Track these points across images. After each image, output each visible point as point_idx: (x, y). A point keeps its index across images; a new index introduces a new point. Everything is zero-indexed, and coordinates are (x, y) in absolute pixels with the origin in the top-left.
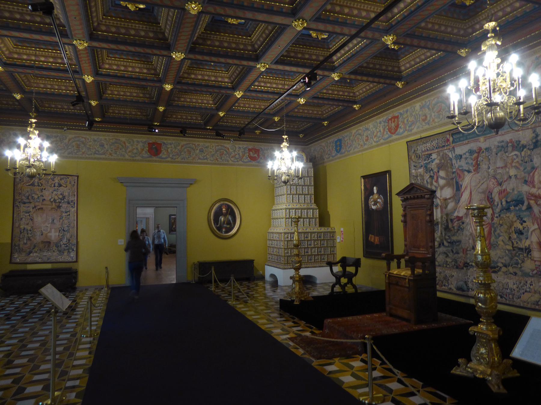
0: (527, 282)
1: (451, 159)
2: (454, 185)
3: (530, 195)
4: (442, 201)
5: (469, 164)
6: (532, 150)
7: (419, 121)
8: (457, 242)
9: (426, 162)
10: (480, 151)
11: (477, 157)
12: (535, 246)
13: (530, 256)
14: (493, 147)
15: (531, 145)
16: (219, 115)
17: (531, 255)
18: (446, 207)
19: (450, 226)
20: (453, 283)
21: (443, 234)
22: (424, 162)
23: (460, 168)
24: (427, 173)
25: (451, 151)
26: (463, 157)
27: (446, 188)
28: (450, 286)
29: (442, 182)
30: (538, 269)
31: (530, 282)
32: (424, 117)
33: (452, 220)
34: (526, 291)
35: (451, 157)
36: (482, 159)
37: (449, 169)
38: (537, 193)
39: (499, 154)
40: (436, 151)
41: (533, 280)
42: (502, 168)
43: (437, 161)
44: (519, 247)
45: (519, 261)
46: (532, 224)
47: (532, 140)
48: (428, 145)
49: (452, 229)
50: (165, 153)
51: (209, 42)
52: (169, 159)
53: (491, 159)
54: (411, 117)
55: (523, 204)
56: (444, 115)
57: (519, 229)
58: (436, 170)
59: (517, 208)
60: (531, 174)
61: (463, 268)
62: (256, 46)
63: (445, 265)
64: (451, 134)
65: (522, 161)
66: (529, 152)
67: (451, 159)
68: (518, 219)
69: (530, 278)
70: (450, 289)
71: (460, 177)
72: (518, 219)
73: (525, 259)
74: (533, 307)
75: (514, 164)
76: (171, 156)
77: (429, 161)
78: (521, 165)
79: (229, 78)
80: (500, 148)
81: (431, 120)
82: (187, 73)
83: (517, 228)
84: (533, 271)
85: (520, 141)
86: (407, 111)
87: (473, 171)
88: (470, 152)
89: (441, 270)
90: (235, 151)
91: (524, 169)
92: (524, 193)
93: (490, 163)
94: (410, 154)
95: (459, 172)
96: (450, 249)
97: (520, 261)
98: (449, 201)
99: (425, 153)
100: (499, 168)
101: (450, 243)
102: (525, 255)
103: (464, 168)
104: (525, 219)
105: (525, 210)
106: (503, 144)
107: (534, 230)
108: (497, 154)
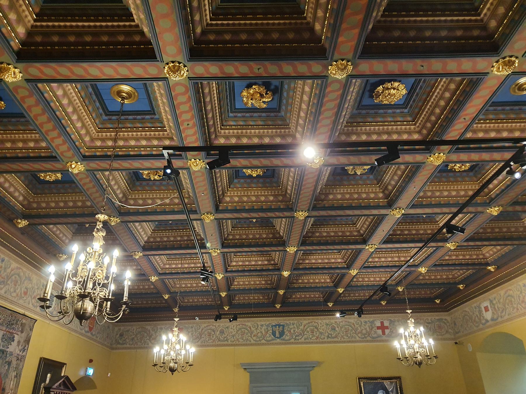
16: (338, 291)
50: (288, 334)
51: (317, 234)
52: (293, 340)
62: (362, 232)
76: (294, 337)
79: (343, 259)
82: (302, 260)
90: (360, 326)
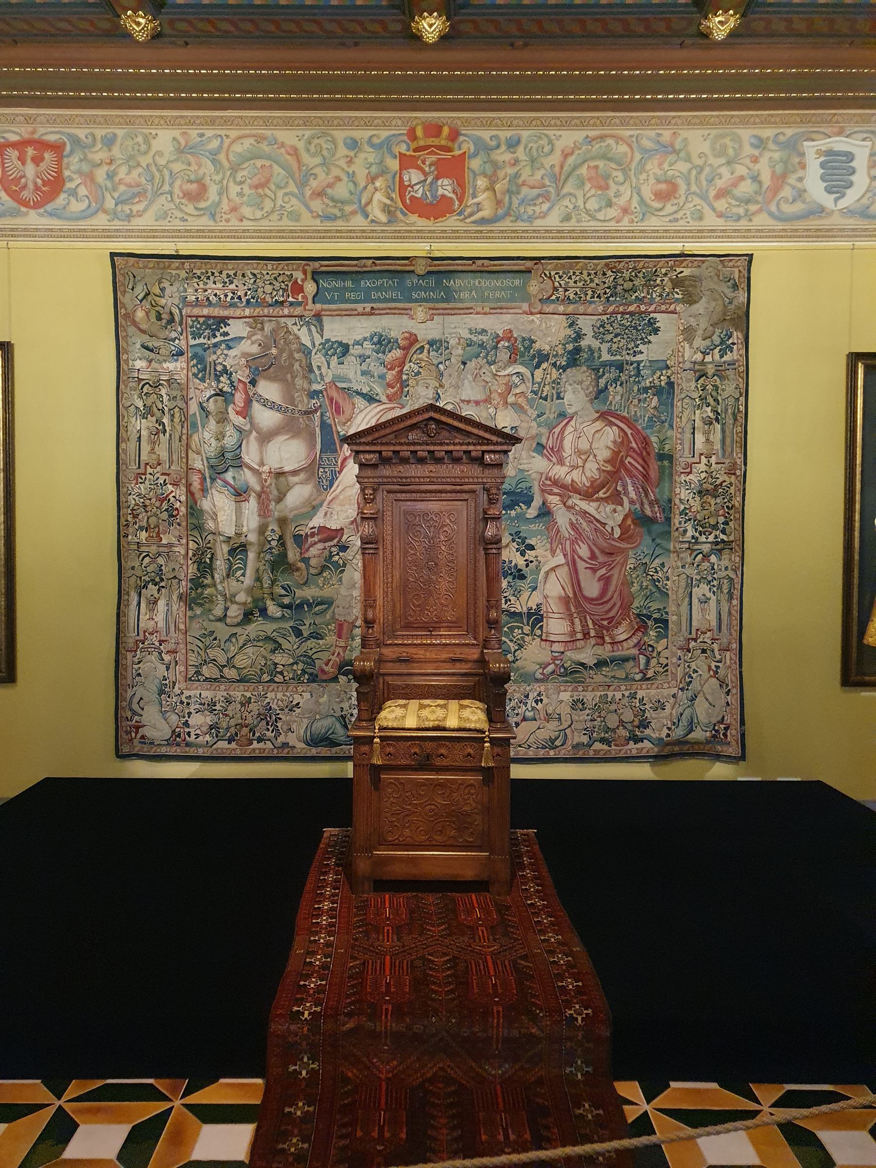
0: (527, 696)
1: (307, 352)
2: (312, 435)
3: (549, 482)
4: (264, 476)
5: (373, 376)
6: (564, 369)
7: (171, 193)
8: (318, 604)
9: (202, 340)
10: (411, 344)
11: (403, 364)
12: (555, 606)
13: (538, 632)
14: (453, 342)
15: (562, 355)
17: (541, 628)
18: (280, 500)
19: (293, 554)
20: (294, 726)
21: (266, 583)
22: (192, 342)
23: (340, 385)
24: (203, 380)
25: (308, 324)
26: (355, 351)
27: (281, 438)
28: (281, 739)
29: (266, 418)
30: (558, 662)
31: (536, 694)
32: (194, 187)
33: (299, 540)
34: (524, 719)
35: (309, 344)
36: (416, 368)
37: (299, 382)
38: (568, 480)
39: (471, 365)
40: (247, 312)
41: (542, 688)
42: (477, 403)
43: (250, 347)
44: (513, 610)
45: (511, 644)
46: (548, 554)
47: (564, 345)
48: (211, 284)
49: (301, 565)
53: (445, 374)
54: (131, 168)
55: (529, 502)
56: (279, 202)
57: (516, 565)
58: (242, 375)
59: (513, 513)
60: (557, 430)
61: (335, 679)
63: (266, 677)
64: (309, 269)
65: (535, 393)
66: (555, 374)
67: (307, 352)
68: (513, 540)
69: (536, 685)
70: (285, 745)
71: (338, 410)
72: (513, 540)
73: (527, 638)
74: (541, 753)
75: (511, 399)
77: (214, 341)
78: (530, 402)
80: (475, 349)
81: (225, 206)
83: (511, 562)
84: (544, 666)
85: (534, 342)
86: (109, 142)
87: (384, 399)
88: (379, 342)
89: (248, 694)
91: (539, 416)
92: (534, 476)
93: (441, 386)
94: (126, 299)
95: (334, 394)
96: (288, 625)
97: (513, 647)
98: (296, 479)
99: (196, 311)
100: (469, 402)
101: (289, 607)
102: (527, 629)
103: (356, 387)
104: (532, 541)
105: (538, 516)
106: (485, 338)
107: (553, 569)
108: (464, 363)
